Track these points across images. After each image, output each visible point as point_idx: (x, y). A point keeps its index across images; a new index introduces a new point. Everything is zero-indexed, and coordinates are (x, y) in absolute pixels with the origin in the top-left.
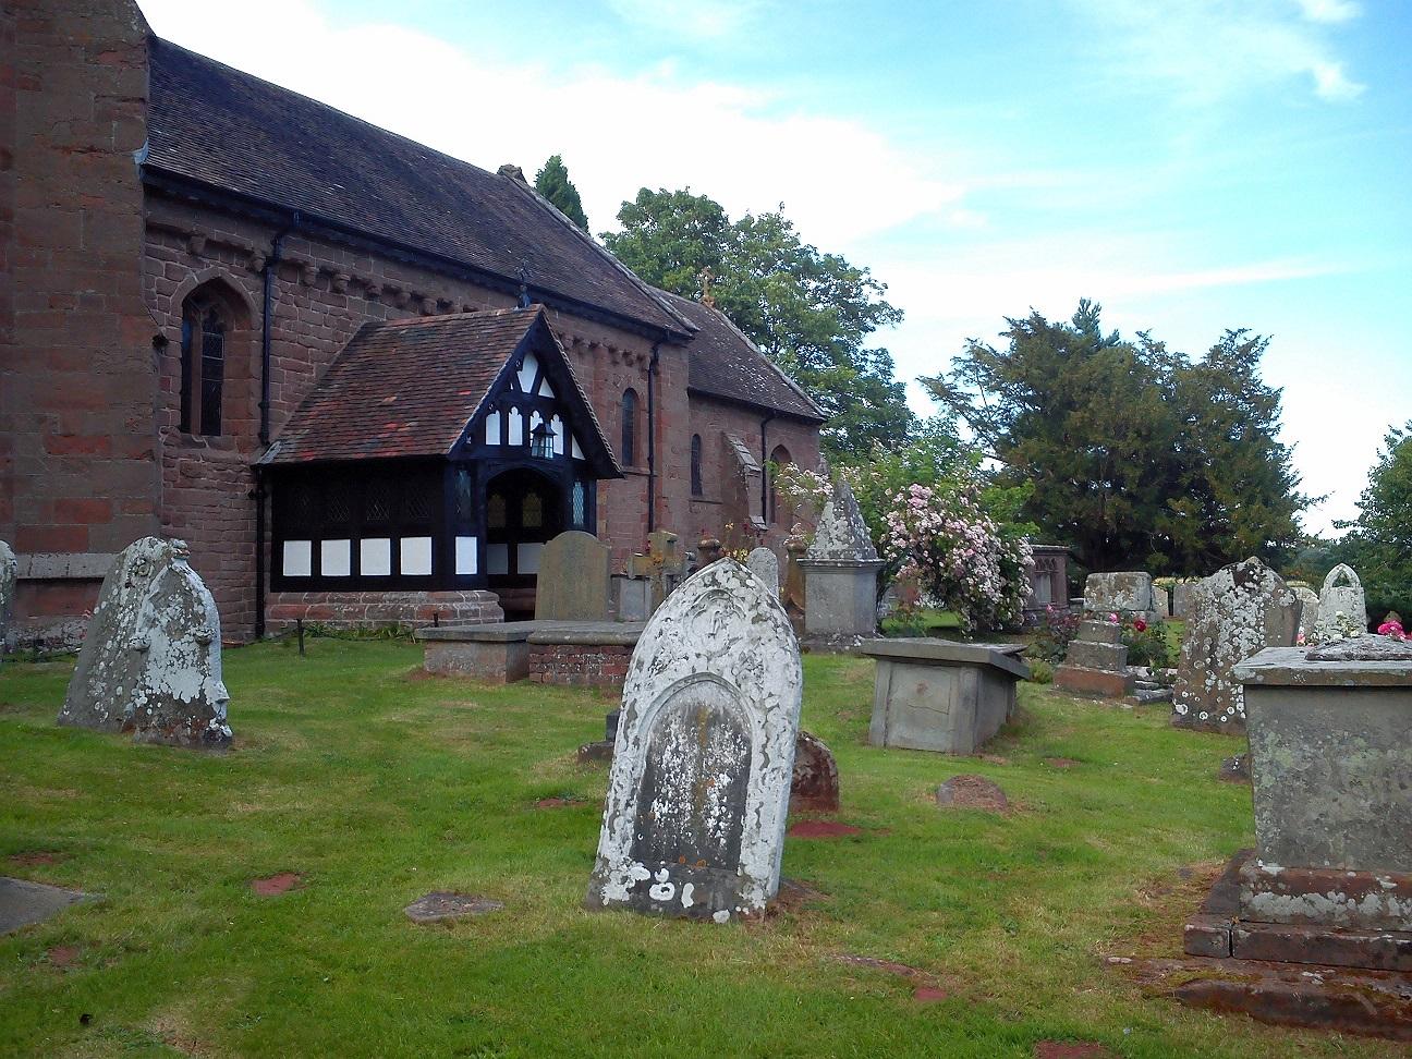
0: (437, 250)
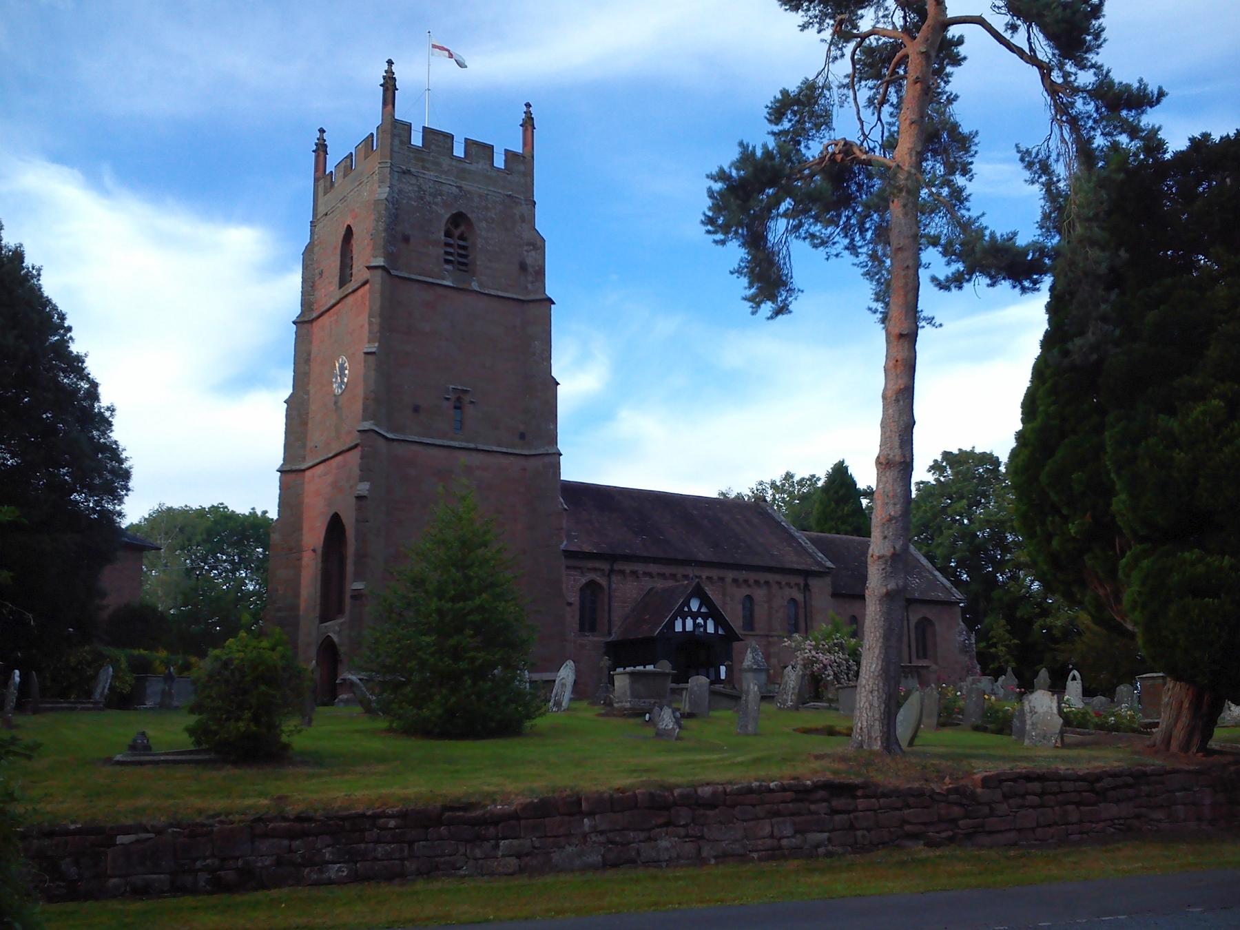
0: (680, 557)
